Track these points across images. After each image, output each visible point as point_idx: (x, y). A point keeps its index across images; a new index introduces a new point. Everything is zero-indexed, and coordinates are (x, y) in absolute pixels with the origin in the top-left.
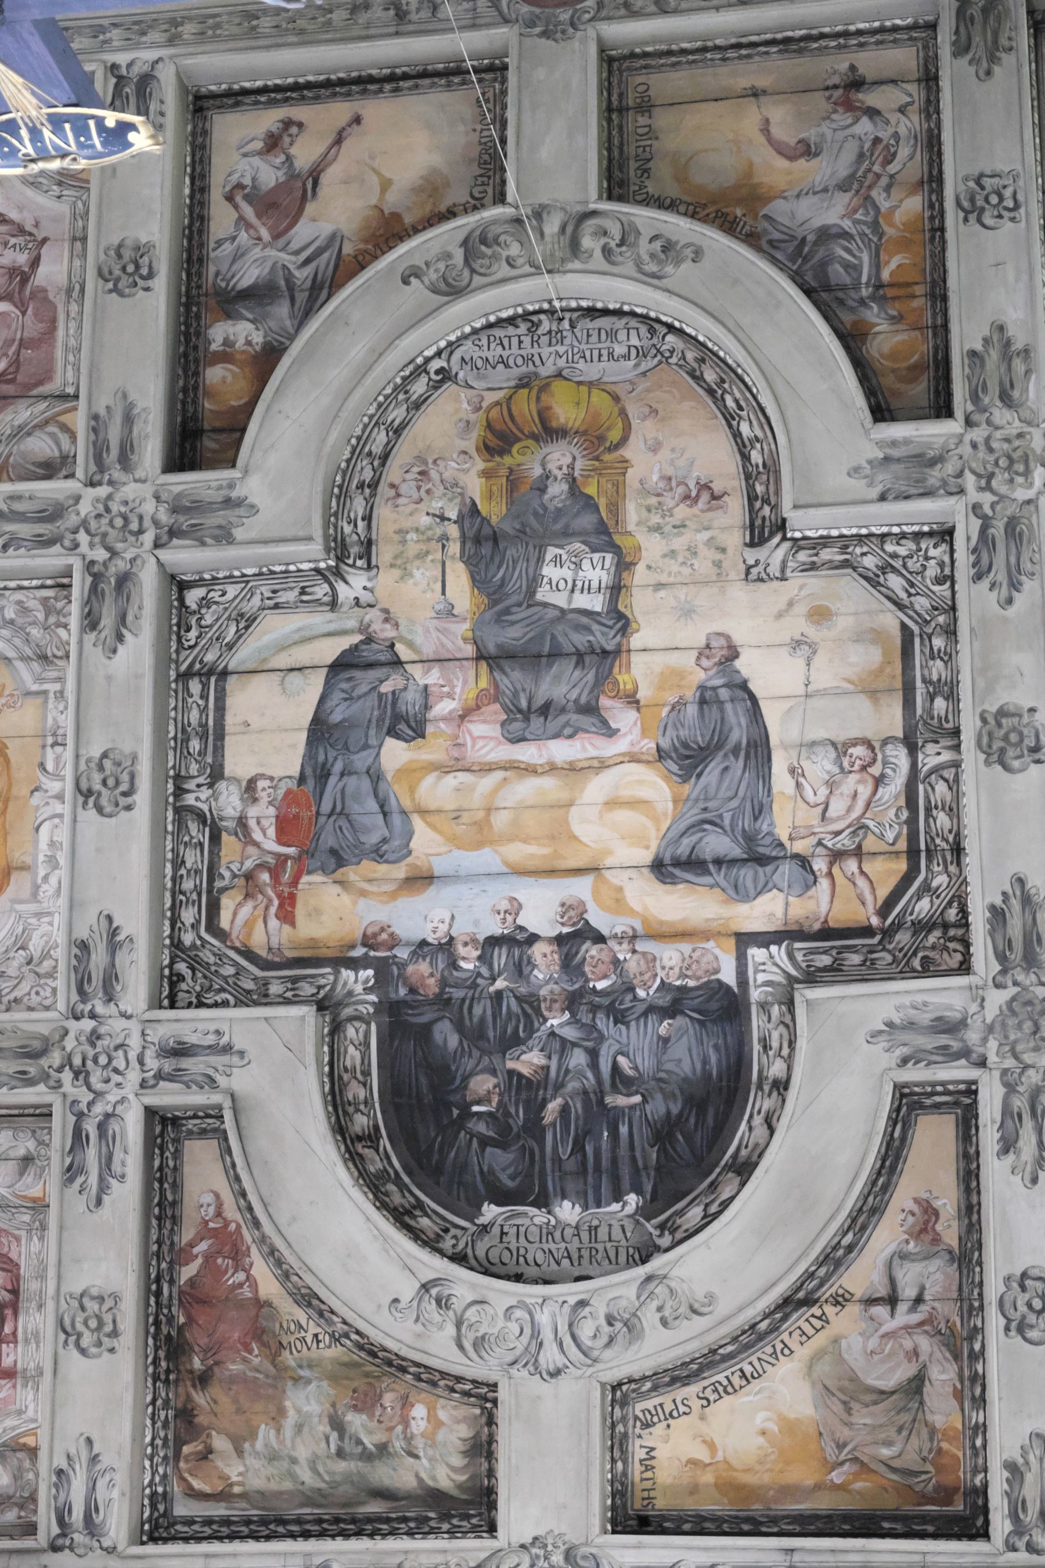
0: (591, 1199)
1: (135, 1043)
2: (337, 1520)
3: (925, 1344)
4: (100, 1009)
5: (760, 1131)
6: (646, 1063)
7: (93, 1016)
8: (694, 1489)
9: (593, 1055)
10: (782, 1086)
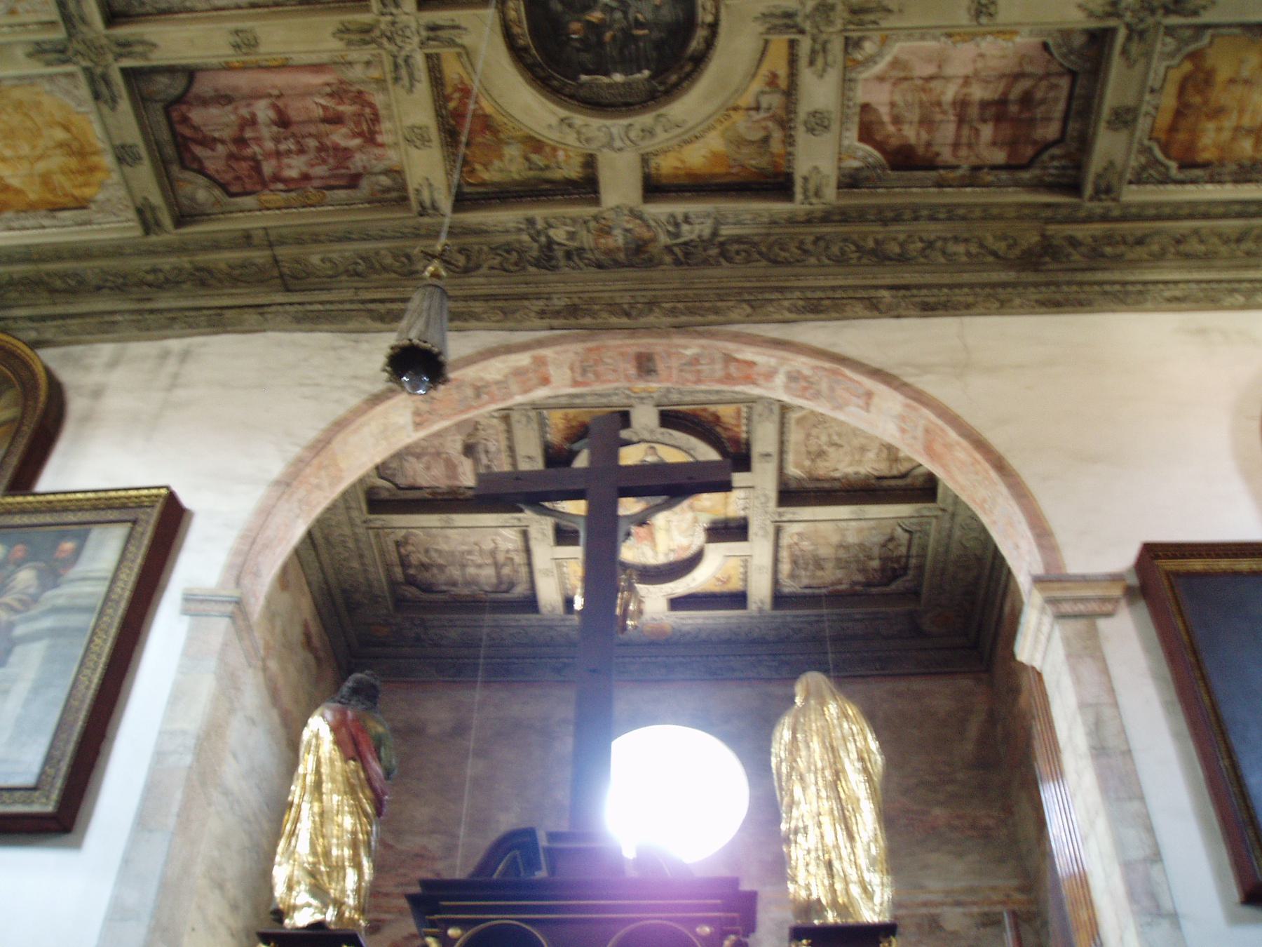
0: (626, 72)
1: (413, 25)
2: (532, 191)
3: (770, 124)
4: (394, 11)
6: (650, 16)
7: (392, 14)
8: (676, 176)
9: (625, 13)
10: (714, 27)
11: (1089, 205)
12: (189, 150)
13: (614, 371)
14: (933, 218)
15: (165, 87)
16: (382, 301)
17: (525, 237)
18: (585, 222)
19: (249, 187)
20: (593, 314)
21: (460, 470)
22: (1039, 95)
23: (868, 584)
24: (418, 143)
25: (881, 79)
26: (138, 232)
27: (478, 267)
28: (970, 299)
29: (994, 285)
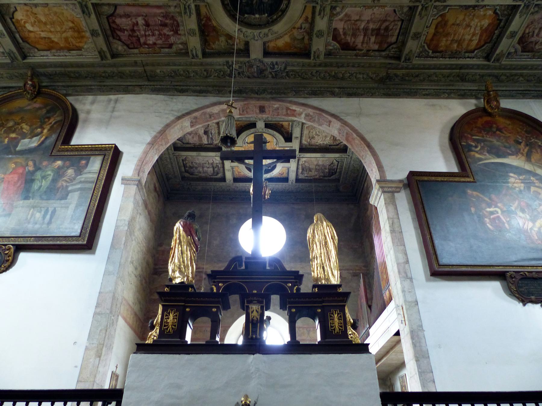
0: (260, 14)
3: (305, 34)
5: (285, 6)
11: (403, 64)
12: (115, 32)
13: (252, 111)
14: (353, 66)
15: (108, 10)
16: (180, 86)
17: (226, 67)
18: (245, 63)
19: (136, 46)
20: (247, 93)
21: (203, 138)
22: (391, 27)
23: (324, 176)
24: (192, 35)
25: (341, 20)
26: (99, 60)
27: (210, 76)
28: (363, 92)
29: (370, 88)
